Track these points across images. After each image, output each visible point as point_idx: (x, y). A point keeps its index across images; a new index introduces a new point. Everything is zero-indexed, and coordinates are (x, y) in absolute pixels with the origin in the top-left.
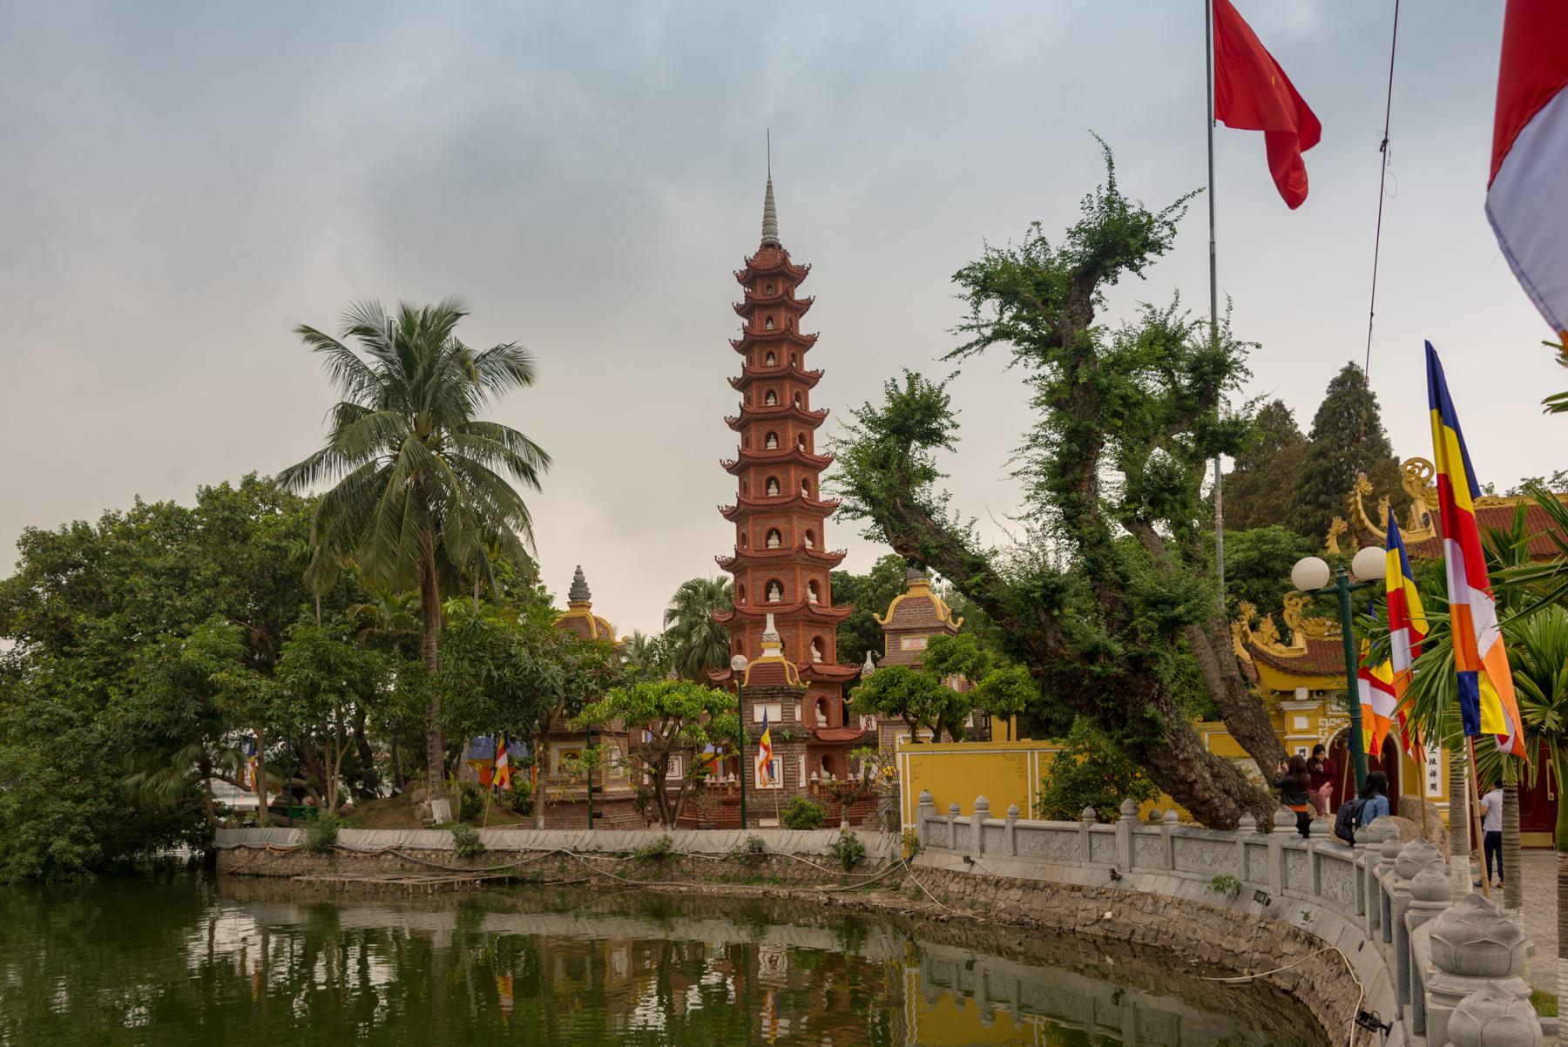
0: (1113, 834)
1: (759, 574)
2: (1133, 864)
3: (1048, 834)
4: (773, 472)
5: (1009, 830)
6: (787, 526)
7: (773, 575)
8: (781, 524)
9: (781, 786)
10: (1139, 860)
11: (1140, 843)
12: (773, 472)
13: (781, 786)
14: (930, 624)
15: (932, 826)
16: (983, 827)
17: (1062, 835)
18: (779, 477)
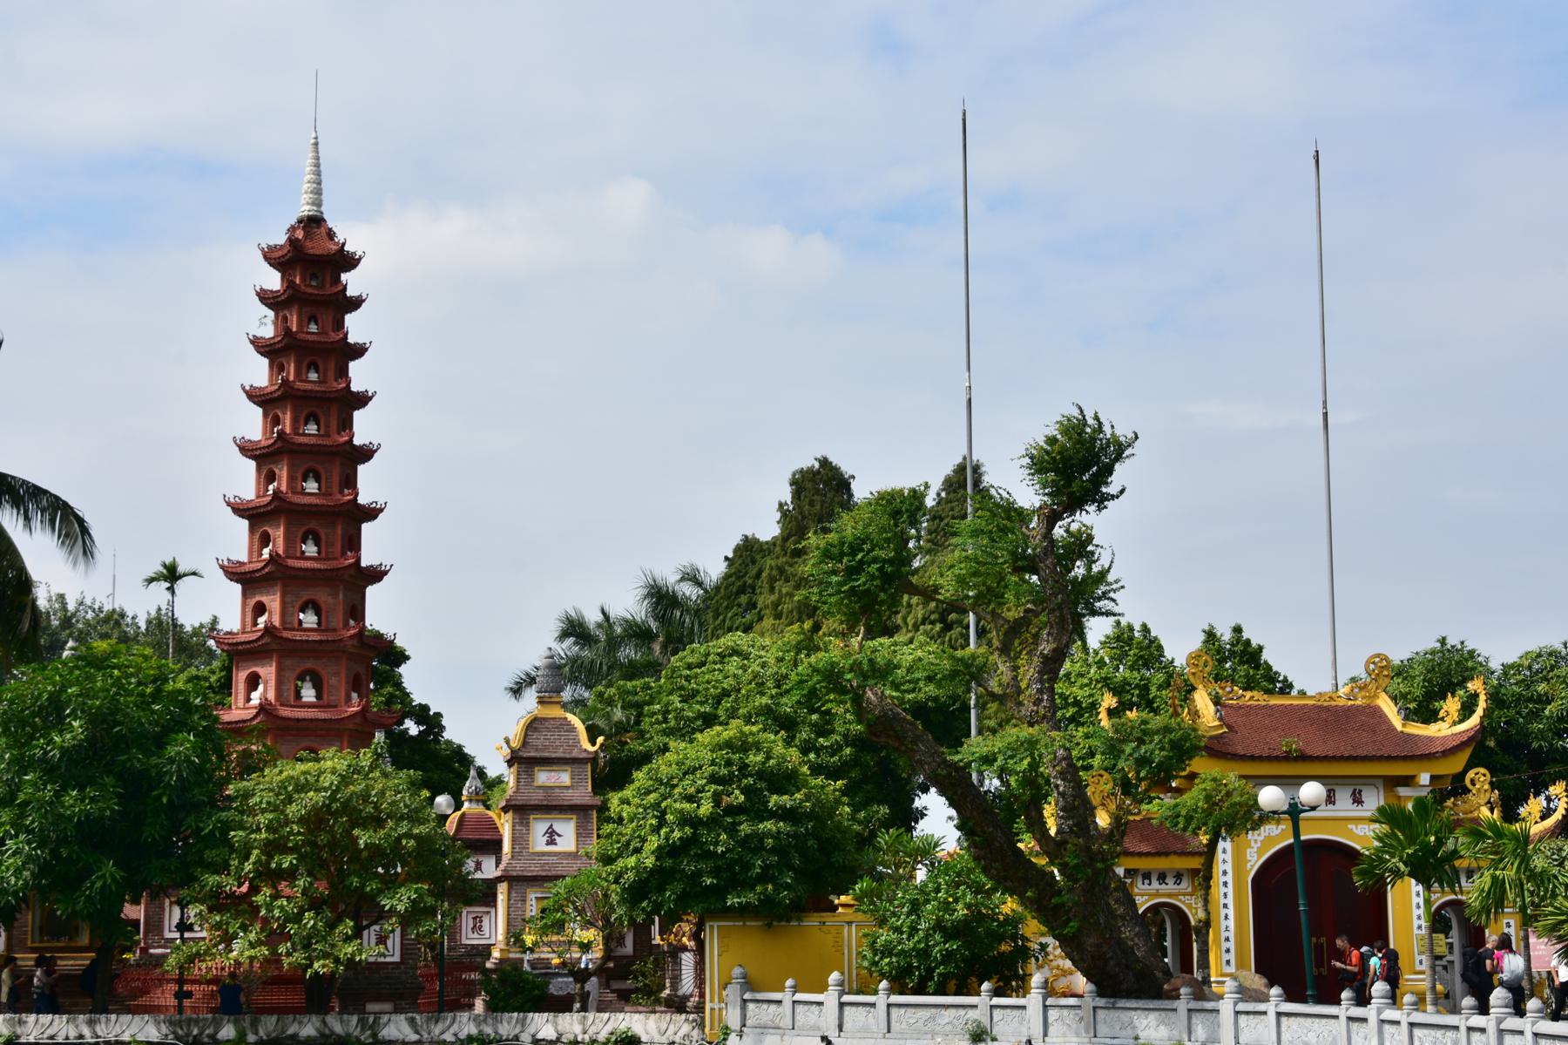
0: (1024, 1007)
1: (288, 662)
2: (1045, 1035)
3: (933, 1011)
4: (313, 525)
5: (882, 1007)
6: (330, 600)
7: (309, 664)
8: (323, 597)
9: (397, 958)
10: (1051, 1030)
11: (1053, 1014)
12: (313, 525)
13: (397, 958)
14: (575, 754)
15: (751, 1006)
16: (842, 1005)
17: (953, 1012)
18: (322, 533)
